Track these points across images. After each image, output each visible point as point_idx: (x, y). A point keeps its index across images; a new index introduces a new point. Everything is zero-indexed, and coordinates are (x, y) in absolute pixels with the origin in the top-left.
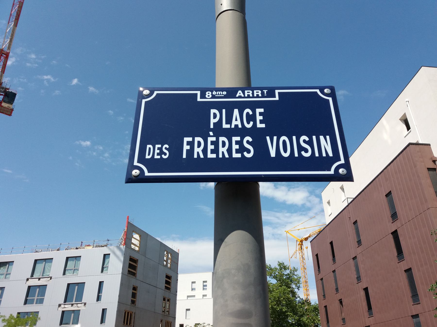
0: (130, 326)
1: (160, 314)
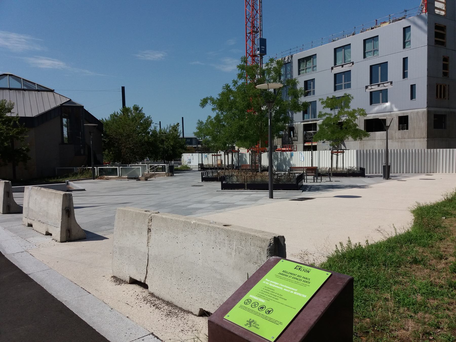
0: (437, 84)
1: (433, 46)
